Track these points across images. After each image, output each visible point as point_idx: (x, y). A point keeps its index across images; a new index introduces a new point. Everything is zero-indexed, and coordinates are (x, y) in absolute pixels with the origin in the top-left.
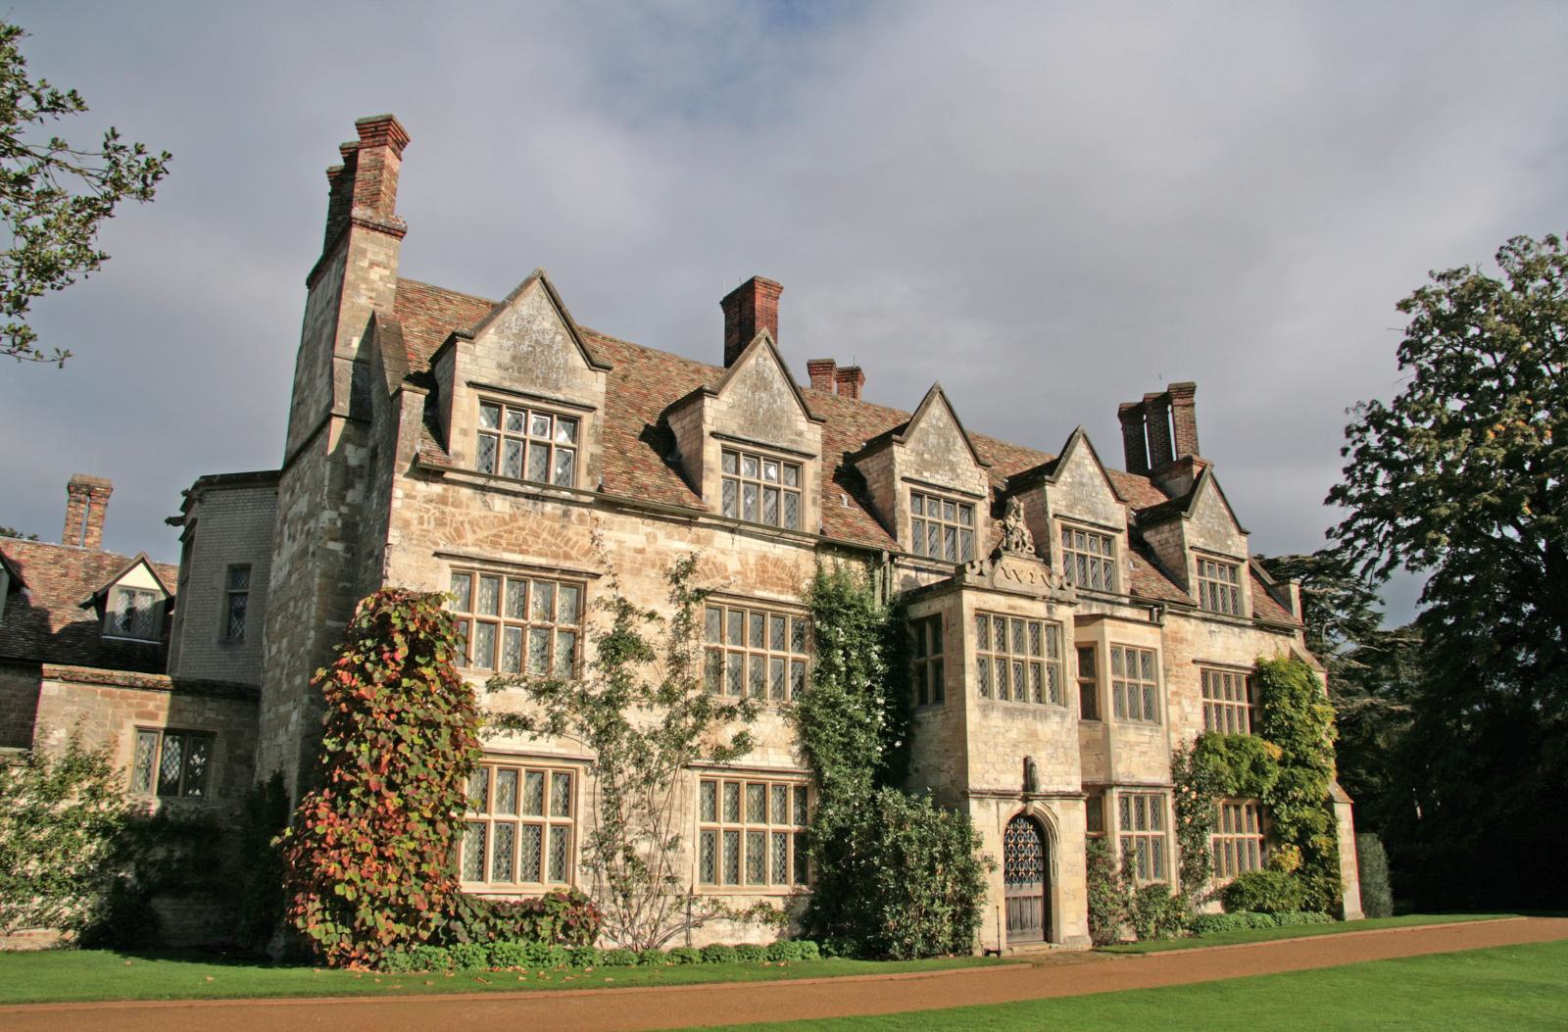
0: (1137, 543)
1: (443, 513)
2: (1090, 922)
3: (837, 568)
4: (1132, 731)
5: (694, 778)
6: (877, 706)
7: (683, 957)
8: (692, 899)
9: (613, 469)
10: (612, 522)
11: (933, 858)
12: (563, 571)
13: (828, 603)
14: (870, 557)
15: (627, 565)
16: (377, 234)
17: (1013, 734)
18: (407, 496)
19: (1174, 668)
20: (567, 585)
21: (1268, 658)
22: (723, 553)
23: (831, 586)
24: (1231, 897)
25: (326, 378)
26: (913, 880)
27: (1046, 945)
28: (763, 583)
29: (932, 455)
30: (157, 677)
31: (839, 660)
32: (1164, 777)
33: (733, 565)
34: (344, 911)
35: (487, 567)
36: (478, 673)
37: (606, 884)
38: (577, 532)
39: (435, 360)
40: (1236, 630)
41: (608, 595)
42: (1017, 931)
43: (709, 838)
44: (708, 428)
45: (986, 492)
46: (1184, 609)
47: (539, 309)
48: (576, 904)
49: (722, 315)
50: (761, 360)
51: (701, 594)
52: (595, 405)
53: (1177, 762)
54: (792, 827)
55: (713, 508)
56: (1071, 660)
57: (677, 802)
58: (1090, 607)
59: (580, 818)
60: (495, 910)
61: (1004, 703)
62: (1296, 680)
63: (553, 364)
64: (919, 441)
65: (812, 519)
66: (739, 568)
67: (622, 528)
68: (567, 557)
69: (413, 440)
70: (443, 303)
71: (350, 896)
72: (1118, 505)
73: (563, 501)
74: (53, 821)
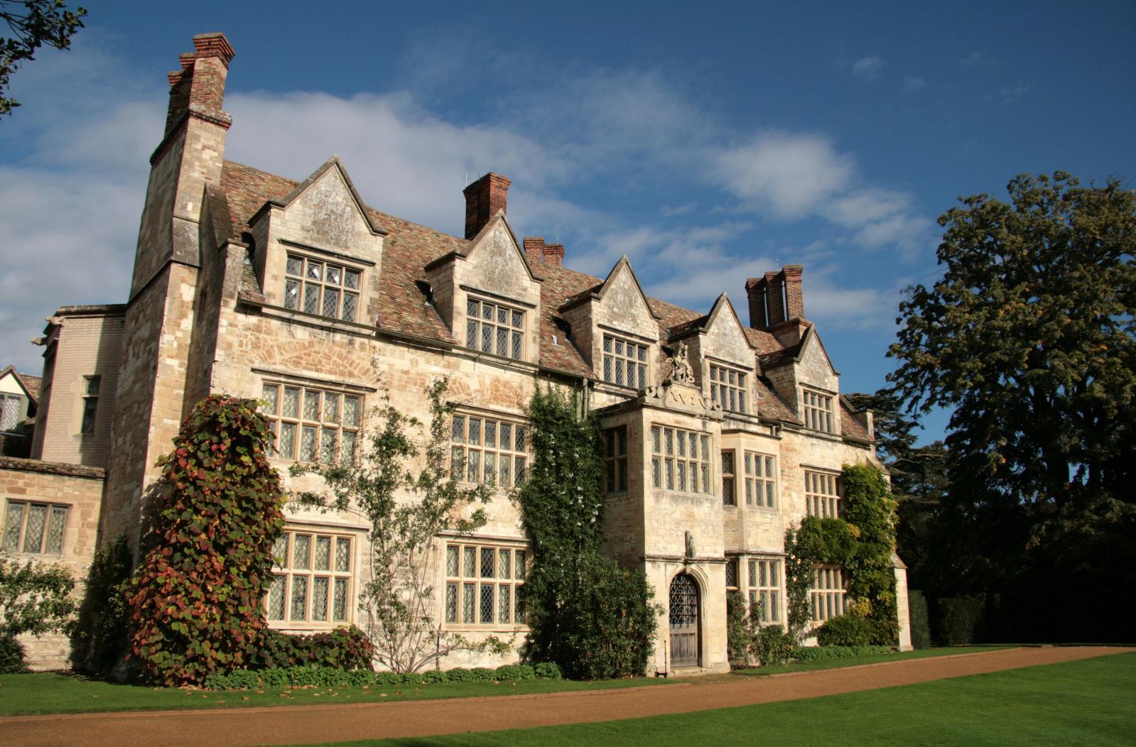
0: (762, 379)
1: (258, 338)
2: (729, 652)
3: (549, 387)
4: (758, 514)
5: (442, 543)
6: (578, 493)
7: (434, 678)
8: (441, 635)
9: (386, 310)
10: (385, 350)
11: (620, 605)
12: (349, 386)
13: (544, 416)
14: (574, 382)
15: (395, 383)
16: (208, 124)
17: (677, 515)
18: (231, 325)
19: (787, 470)
21: (852, 464)
22: (467, 376)
23: (546, 402)
24: (823, 634)
25: (166, 233)
26: (607, 621)
27: (698, 669)
28: (496, 399)
29: (619, 309)
30: (26, 461)
31: (551, 458)
32: (780, 549)
33: (474, 385)
34: (177, 643)
35: (291, 381)
36: (281, 462)
37: (379, 623)
39: (252, 222)
40: (830, 443)
41: (382, 405)
42: (678, 659)
43: (453, 587)
44: (457, 281)
46: (795, 427)
47: (334, 186)
48: (357, 638)
49: (464, 201)
50: (497, 233)
51: (451, 406)
52: (375, 261)
53: (789, 538)
54: (514, 582)
55: (460, 342)
56: (716, 462)
57: (430, 561)
58: (729, 424)
59: (358, 572)
60: (295, 641)
62: (870, 481)
63: (343, 229)
64: (610, 298)
66: (479, 388)
67: (392, 354)
68: (351, 375)
69: (236, 281)
70: (257, 180)
71: (182, 628)
72: (750, 351)
73: (348, 333)
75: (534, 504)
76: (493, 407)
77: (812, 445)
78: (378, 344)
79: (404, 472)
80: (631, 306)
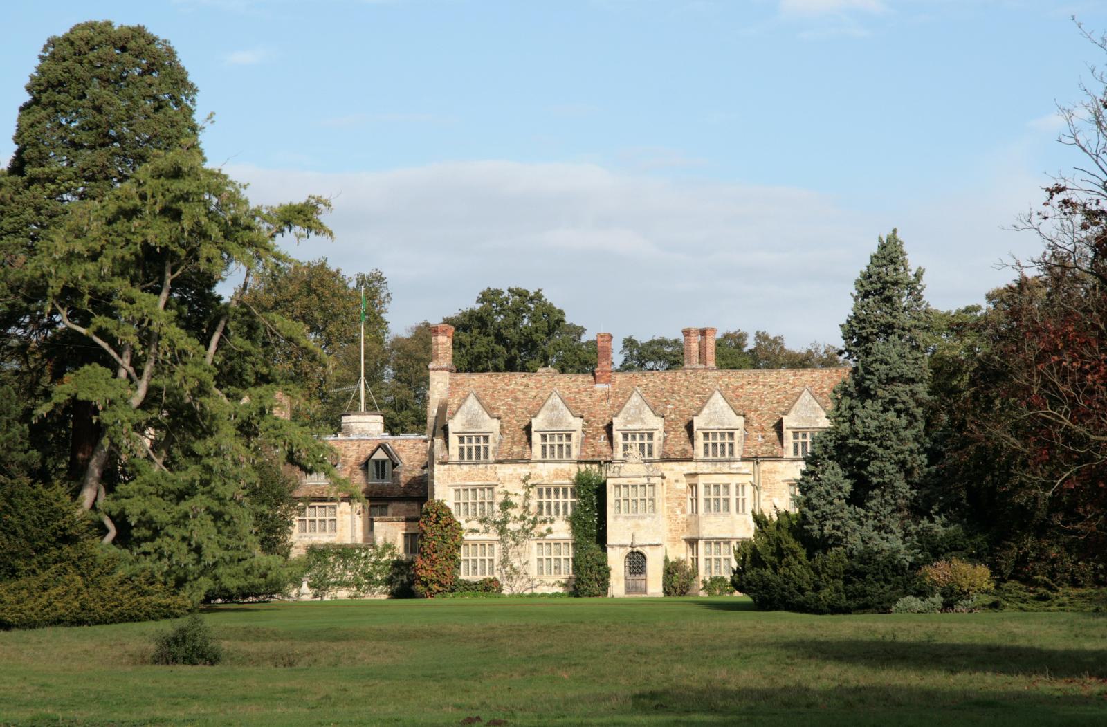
5: (534, 544)
14: (598, 462)
20: (489, 489)
28: (557, 478)
33: (545, 474)
34: (426, 584)
41: (501, 490)
43: (540, 560)
44: (533, 430)
46: (778, 458)
51: (533, 485)
54: (571, 556)
65: (575, 453)
75: (576, 522)
76: (555, 482)
79: (513, 515)
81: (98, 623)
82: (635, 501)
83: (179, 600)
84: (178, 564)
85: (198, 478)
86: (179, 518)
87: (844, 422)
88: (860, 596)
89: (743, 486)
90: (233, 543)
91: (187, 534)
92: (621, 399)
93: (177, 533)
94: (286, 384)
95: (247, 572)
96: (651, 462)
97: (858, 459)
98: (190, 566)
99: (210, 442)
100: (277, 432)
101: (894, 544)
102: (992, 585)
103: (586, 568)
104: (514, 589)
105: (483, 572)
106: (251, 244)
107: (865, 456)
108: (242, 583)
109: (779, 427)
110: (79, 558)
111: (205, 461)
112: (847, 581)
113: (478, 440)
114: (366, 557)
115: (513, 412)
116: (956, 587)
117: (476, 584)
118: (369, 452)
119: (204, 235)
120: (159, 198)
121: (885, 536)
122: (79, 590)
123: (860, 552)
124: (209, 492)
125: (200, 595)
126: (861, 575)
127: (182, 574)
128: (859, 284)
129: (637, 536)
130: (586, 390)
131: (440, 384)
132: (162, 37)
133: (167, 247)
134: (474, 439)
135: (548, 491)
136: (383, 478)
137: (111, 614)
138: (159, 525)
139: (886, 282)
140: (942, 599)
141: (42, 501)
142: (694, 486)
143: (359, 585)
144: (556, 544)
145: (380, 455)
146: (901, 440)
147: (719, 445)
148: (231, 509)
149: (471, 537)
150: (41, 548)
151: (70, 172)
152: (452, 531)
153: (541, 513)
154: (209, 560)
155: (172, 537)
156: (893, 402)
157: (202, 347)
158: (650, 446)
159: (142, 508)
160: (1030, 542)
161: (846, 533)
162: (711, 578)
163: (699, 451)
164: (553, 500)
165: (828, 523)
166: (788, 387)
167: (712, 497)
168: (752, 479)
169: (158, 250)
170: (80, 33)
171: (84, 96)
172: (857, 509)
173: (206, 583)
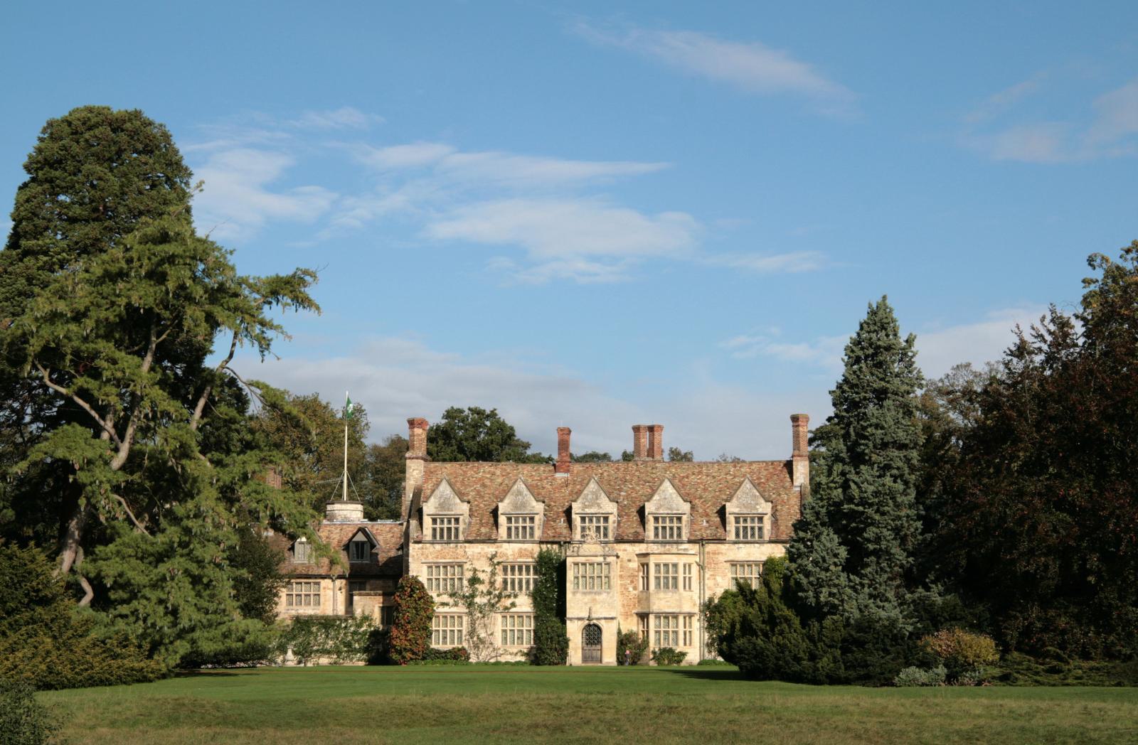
5: (499, 617)
14: (558, 543)
17: (586, 600)
20: (459, 566)
28: (521, 557)
33: (510, 552)
34: (400, 652)
38: (460, 551)
40: (757, 545)
41: (470, 567)
43: (504, 631)
44: (500, 512)
45: (615, 511)
46: (721, 541)
51: (499, 563)
54: (532, 628)
61: (585, 590)
65: (538, 534)
74: (360, 634)
75: (538, 597)
76: (519, 560)
77: (738, 548)
78: (467, 545)
80: (597, 499)
81: (64, 687)
82: (592, 578)
83: (153, 664)
84: (154, 625)
85: (177, 540)
86: (158, 581)
87: (836, 488)
88: (859, 666)
89: (690, 566)
90: (212, 607)
91: (164, 597)
92: (578, 487)
93: (154, 595)
94: (269, 451)
95: (225, 636)
96: (606, 543)
97: (854, 525)
98: (166, 628)
99: (190, 504)
100: (259, 497)
101: (889, 612)
102: (997, 656)
103: (547, 639)
104: (481, 657)
105: (452, 642)
106: (236, 309)
107: (861, 522)
108: (219, 647)
109: (722, 513)
110: (52, 620)
111: (186, 523)
112: (845, 651)
113: (449, 522)
114: (346, 627)
115: (482, 497)
116: (960, 658)
117: (445, 652)
118: (350, 535)
119: (190, 299)
120: (146, 261)
121: (882, 604)
122: (48, 652)
123: (856, 621)
124: (188, 555)
125: (174, 660)
126: (860, 644)
127: (157, 637)
128: (849, 350)
129: (593, 610)
130: (547, 478)
131: (415, 471)
132: (157, 121)
133: (151, 309)
134: (446, 520)
135: (513, 568)
136: (362, 557)
137: (80, 678)
138: (136, 587)
139: (879, 347)
140: (946, 670)
141: (15, 562)
142: (645, 566)
143: (339, 653)
144: (519, 617)
145: (360, 537)
146: (898, 506)
147: (668, 528)
148: (210, 571)
149: (441, 609)
150: (13, 610)
151: (64, 244)
152: (424, 603)
153: (505, 589)
154: (184, 623)
155: (148, 599)
156: (887, 467)
157: (185, 411)
158: (606, 529)
159: (120, 569)
160: (1035, 612)
161: (842, 601)
162: (660, 649)
163: (650, 534)
164: (517, 576)
165: (824, 590)
166: (729, 477)
167: (662, 575)
168: (698, 560)
169: (142, 311)
170: (78, 115)
171: (80, 171)
172: (852, 577)
173: (183, 647)
